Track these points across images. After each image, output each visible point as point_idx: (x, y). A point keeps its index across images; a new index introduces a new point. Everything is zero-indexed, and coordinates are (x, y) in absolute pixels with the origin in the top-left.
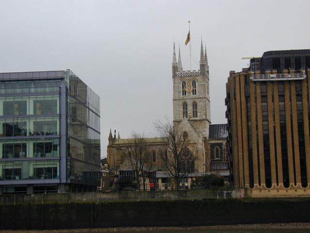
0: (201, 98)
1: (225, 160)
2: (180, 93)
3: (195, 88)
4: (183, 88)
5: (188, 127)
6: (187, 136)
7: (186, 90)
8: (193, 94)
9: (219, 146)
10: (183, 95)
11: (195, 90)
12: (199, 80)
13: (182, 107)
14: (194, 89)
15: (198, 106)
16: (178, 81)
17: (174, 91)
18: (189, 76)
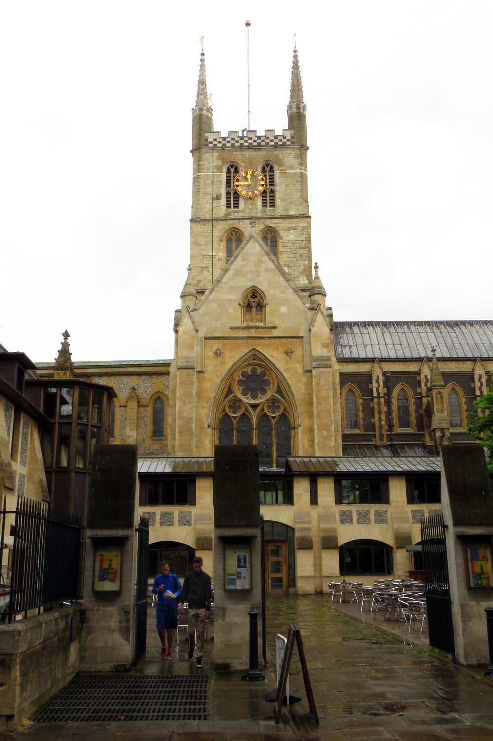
0: (292, 217)
1: (381, 436)
2: (218, 197)
3: (272, 183)
4: (228, 183)
5: (267, 270)
6: (260, 307)
7: (239, 189)
8: (264, 205)
9: (359, 385)
10: (228, 206)
11: (272, 191)
12: (289, 157)
13: (223, 244)
15: (280, 244)
16: (211, 160)
17: (197, 192)
18: (250, 147)
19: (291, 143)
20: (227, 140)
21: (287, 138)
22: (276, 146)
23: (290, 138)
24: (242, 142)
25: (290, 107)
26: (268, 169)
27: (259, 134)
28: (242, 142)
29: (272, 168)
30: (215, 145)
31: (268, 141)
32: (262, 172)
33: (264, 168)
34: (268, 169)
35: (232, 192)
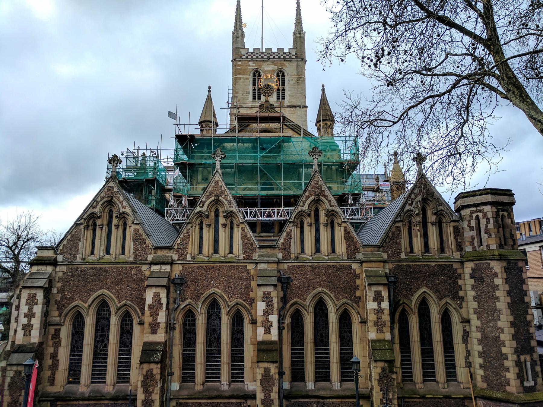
3: (283, 84)
4: (254, 84)
11: (283, 90)
14: (281, 88)
19: (296, 57)
20: (254, 54)
21: (292, 54)
22: (285, 59)
23: (294, 54)
24: (263, 55)
25: (294, 34)
26: (281, 74)
27: (273, 51)
28: (263, 55)
29: (283, 73)
30: (247, 57)
31: (279, 55)
32: (277, 76)
33: (278, 74)
34: (281, 74)
35: (257, 89)
